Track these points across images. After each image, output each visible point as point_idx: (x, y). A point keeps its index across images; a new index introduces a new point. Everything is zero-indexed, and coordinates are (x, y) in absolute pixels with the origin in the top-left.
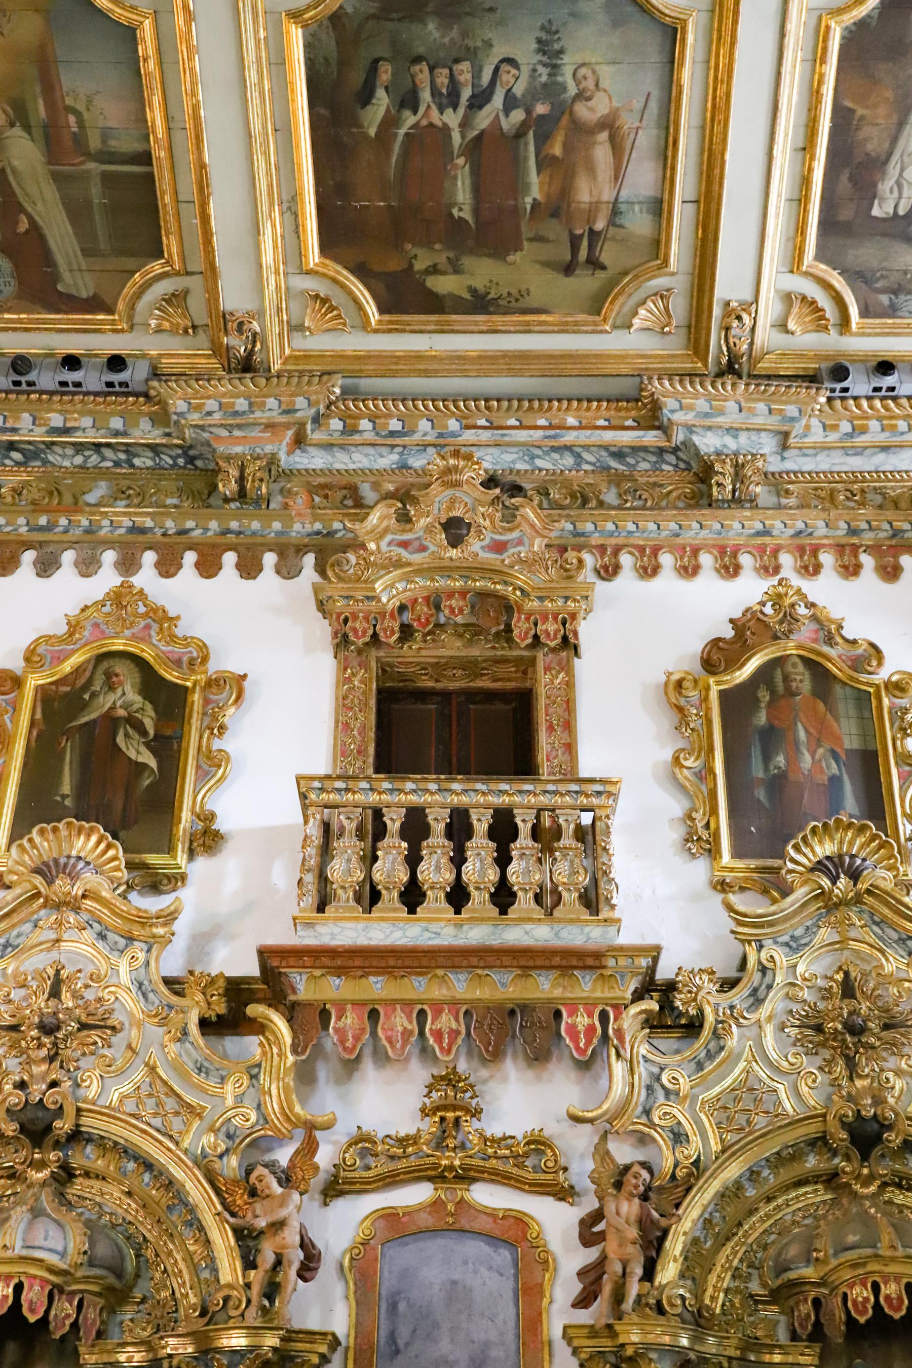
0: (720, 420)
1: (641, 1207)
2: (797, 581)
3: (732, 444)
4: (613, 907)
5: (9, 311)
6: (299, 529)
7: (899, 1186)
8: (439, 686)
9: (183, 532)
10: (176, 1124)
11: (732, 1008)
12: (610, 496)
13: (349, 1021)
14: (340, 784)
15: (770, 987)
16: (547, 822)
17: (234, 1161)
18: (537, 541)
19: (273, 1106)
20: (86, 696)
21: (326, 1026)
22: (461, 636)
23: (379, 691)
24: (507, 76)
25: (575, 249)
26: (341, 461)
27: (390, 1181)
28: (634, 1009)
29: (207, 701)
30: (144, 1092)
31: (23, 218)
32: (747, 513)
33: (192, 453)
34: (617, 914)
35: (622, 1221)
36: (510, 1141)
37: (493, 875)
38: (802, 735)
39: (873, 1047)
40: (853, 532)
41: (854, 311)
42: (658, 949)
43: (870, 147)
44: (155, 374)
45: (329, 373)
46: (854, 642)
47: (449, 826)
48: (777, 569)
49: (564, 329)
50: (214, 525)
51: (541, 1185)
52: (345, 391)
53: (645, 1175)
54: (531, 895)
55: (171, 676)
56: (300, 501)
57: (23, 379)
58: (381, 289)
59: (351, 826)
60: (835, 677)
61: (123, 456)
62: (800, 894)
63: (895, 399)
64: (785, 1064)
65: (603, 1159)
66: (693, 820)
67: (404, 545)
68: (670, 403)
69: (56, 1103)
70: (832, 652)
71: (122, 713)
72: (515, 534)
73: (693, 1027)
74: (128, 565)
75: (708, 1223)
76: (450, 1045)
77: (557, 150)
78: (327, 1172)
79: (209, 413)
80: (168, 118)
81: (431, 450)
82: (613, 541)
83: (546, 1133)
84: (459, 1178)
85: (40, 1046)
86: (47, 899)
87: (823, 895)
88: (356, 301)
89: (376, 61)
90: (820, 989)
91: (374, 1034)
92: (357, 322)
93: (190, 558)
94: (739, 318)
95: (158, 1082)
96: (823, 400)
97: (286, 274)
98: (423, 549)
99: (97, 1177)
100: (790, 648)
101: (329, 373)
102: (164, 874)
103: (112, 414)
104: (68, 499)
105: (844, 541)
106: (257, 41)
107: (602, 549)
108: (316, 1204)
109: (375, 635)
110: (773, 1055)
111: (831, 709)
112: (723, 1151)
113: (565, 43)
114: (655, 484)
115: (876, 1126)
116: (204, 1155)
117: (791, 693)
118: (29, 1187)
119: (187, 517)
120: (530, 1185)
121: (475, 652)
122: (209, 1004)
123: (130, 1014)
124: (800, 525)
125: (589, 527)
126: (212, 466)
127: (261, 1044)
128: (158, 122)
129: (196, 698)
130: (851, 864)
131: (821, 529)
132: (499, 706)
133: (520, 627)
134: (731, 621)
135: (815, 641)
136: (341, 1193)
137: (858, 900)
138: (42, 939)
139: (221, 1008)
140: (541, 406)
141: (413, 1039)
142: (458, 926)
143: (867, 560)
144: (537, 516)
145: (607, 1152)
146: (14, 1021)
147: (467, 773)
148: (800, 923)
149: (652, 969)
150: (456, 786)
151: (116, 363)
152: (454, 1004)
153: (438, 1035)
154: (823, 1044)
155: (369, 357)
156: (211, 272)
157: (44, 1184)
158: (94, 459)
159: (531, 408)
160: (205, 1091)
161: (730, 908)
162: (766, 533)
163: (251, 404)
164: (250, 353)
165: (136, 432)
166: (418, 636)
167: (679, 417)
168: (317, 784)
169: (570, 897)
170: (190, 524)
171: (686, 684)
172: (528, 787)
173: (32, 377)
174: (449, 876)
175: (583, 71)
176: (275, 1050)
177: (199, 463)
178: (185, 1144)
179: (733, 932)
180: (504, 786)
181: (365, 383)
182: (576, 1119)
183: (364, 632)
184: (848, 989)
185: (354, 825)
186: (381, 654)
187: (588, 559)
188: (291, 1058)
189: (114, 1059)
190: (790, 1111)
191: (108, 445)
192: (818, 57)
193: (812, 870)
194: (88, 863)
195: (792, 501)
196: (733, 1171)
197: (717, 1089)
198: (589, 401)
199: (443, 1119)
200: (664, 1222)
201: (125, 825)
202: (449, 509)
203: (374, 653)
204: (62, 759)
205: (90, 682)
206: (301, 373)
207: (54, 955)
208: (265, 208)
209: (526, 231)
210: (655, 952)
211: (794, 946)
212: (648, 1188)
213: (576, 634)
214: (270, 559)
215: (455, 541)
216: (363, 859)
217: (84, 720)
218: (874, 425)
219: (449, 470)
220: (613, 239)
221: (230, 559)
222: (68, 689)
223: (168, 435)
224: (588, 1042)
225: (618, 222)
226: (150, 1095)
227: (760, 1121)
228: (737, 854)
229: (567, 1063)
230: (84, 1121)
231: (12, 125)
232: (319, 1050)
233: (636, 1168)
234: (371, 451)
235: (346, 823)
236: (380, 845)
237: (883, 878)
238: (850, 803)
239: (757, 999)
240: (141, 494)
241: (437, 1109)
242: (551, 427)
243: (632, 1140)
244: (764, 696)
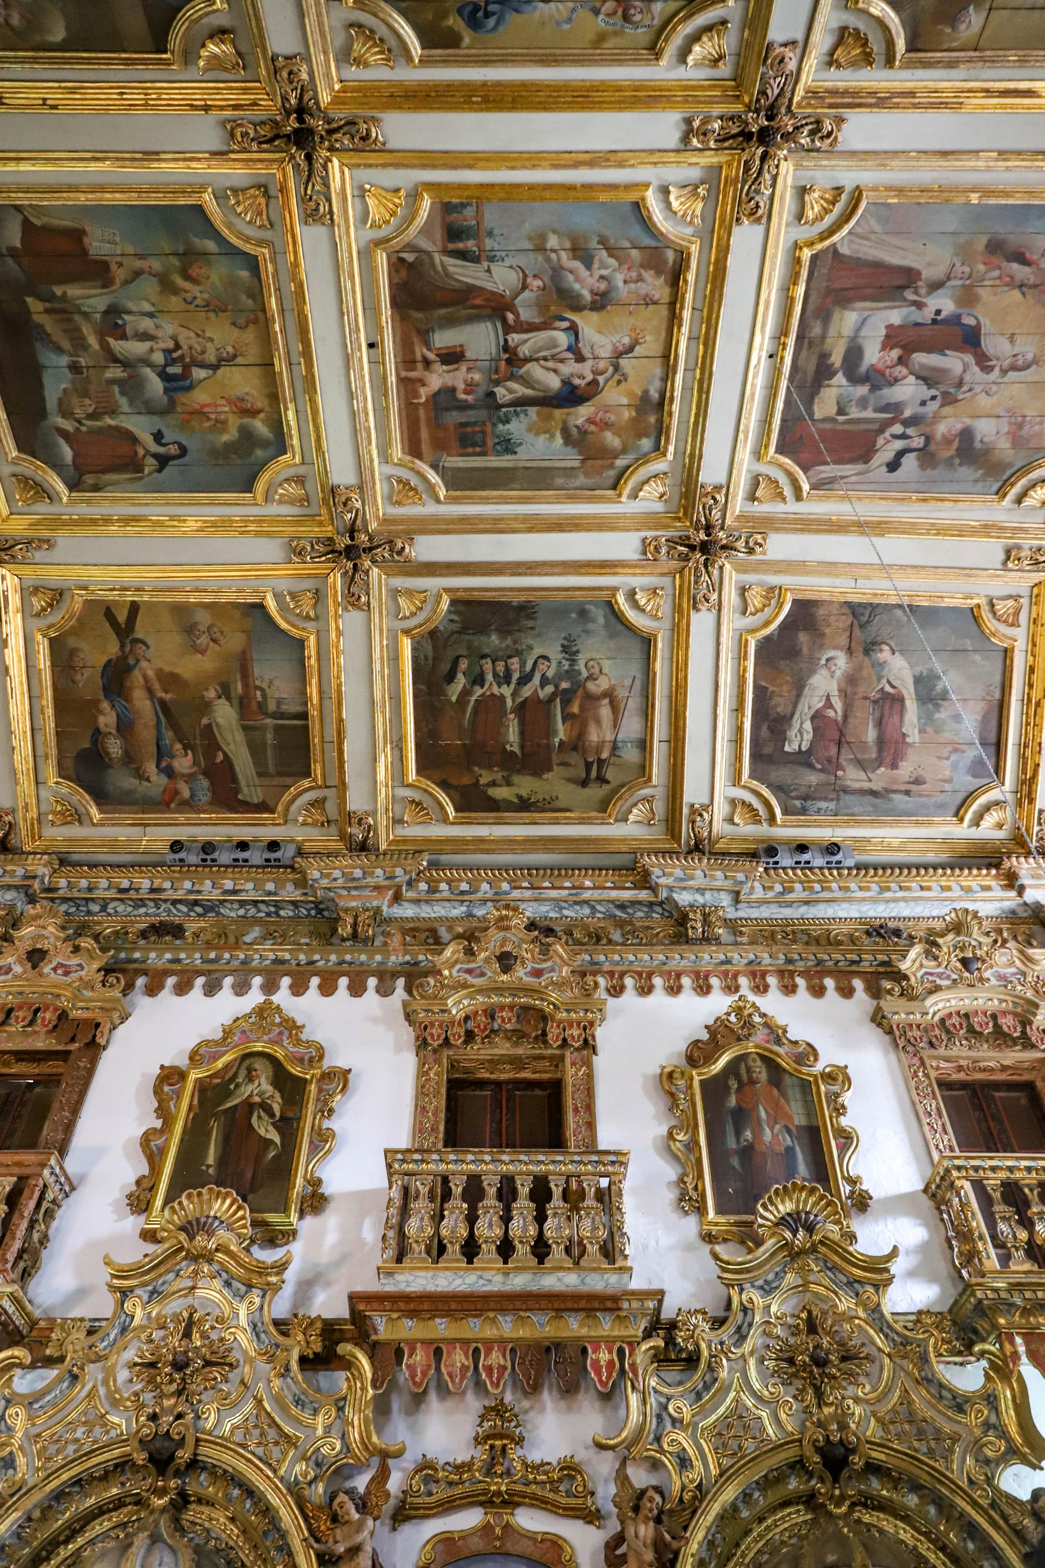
0: (691, 883)
1: (656, 1529)
2: (752, 997)
3: (701, 900)
4: (626, 1257)
5: (204, 812)
6: (395, 959)
7: (865, 1506)
8: (493, 1077)
9: (311, 963)
10: (276, 1452)
11: (722, 1343)
12: (616, 936)
13: (418, 1358)
14: (417, 1157)
15: (750, 1325)
16: (574, 1186)
17: (320, 1488)
18: (565, 969)
19: (354, 1435)
20: (232, 1087)
21: (399, 1362)
22: (509, 1039)
23: (449, 1081)
24: (542, 666)
25: (588, 771)
26: (426, 912)
27: (448, 1507)
28: (644, 1347)
29: (320, 1090)
30: (250, 1424)
31: (220, 754)
32: (714, 948)
33: (321, 906)
34: (629, 1263)
35: (641, 1544)
36: (547, 1467)
37: (532, 1231)
38: (763, 1114)
39: (835, 1377)
40: (789, 961)
41: (778, 811)
42: (662, 1293)
43: (779, 710)
44: (300, 853)
45: (420, 852)
46: (796, 1043)
47: (499, 1190)
48: (737, 989)
49: (582, 821)
50: (333, 958)
51: (573, 1509)
52: (432, 864)
53: (658, 1498)
54: (562, 1247)
55: (295, 1070)
56: (396, 940)
57: (209, 857)
58: (457, 796)
59: (424, 1190)
60: (784, 1070)
61: (272, 909)
62: (769, 1244)
63: (811, 869)
64: (766, 1393)
65: (623, 1484)
66: (685, 1183)
67: (469, 971)
68: (657, 872)
69: (179, 1434)
70: (780, 1050)
71: (257, 1099)
72: (549, 964)
73: (692, 1361)
74: (270, 987)
75: (711, 1544)
76: (499, 1379)
77: (575, 709)
78: (396, 1497)
79: (335, 879)
80: (321, 692)
81: (489, 904)
82: (619, 968)
83: (576, 1459)
84: (505, 1503)
85: (171, 1381)
86: (188, 1251)
87: (787, 1246)
88: (440, 804)
89: (458, 657)
90: (790, 1326)
91: (438, 1369)
92: (440, 817)
93: (315, 981)
94: (701, 815)
95: (263, 1413)
96: (761, 869)
97: (393, 787)
98: (483, 974)
99: (208, 1503)
100: (750, 1047)
101: (420, 852)
102: (281, 1231)
103: (268, 880)
104: (232, 940)
105: (784, 968)
106: (382, 647)
107: (611, 974)
108: (387, 1529)
109: (446, 1039)
110: (757, 1386)
111: (783, 1094)
112: (721, 1475)
113: (579, 647)
114: (648, 928)
115: (842, 1450)
116: (297, 1482)
117: (752, 1082)
118: (152, 1512)
119: (314, 951)
120: (564, 1509)
121: (520, 1051)
122: (308, 1343)
123: (245, 1352)
124: (752, 957)
125: (602, 958)
126: (334, 915)
127: (348, 1379)
128: (314, 695)
129: (313, 1087)
130: (806, 1220)
131: (766, 960)
132: (538, 1092)
133: (553, 1032)
134: (706, 1027)
135: (768, 1042)
136: (408, 1518)
137: (814, 1249)
138: (181, 1286)
139: (317, 1347)
140: (566, 874)
141: (469, 1374)
142: (506, 1274)
143: (800, 982)
144: (565, 951)
145: (627, 1477)
146: (152, 1359)
147: (514, 1147)
148: (771, 1269)
149: (658, 1310)
150: (505, 1158)
151: (273, 846)
152: (502, 1342)
153: (489, 1369)
154: (795, 1375)
155: (448, 840)
156: (342, 786)
157: (163, 1510)
158: (252, 911)
159: (559, 875)
160: (300, 1422)
161: (716, 1257)
162: (728, 962)
163: (364, 873)
164: (366, 839)
165: (283, 893)
166: (478, 1039)
167: (663, 881)
168: (399, 1156)
169: (593, 1249)
170: (316, 957)
171: (675, 1075)
172: (560, 1158)
173: (215, 856)
174: (498, 1231)
175: (591, 663)
176: (359, 1385)
177: (326, 913)
178: (282, 1472)
179: (719, 1277)
180: (541, 1158)
181: (444, 858)
182: (601, 1447)
183: (439, 1036)
184: (812, 1327)
185: (427, 1189)
186: (451, 1053)
187: (601, 981)
188: (371, 1392)
189: (229, 1394)
190: (774, 1438)
191: (263, 902)
192: (741, 655)
193: (777, 1225)
194: (222, 1222)
195: (745, 939)
196: (730, 1494)
197: (714, 1417)
198: (600, 870)
199: (492, 1447)
200: (675, 1545)
201: (253, 1190)
202: (502, 946)
203: (446, 1052)
204: (209, 1135)
205: (235, 1075)
206: (400, 852)
207: (190, 1300)
208: (381, 745)
209: (555, 758)
210: (659, 1295)
211: (767, 1289)
212: (661, 1512)
213: (594, 1039)
214: (372, 982)
215: (506, 969)
216: (432, 1217)
217: (228, 1105)
218: (798, 886)
219: (502, 918)
220: (614, 764)
221: (343, 982)
222: (218, 1081)
223: (305, 894)
224: (609, 1377)
226: (256, 1426)
227: (749, 1445)
228: (719, 1211)
229: (592, 1392)
230: (202, 1450)
231: (219, 697)
232: (393, 1384)
233: (651, 1493)
234: (447, 904)
235: (420, 1187)
236: (446, 1206)
237: (833, 1231)
238: (802, 1168)
239: (741, 1337)
240: (283, 936)
241: (488, 1437)
242: (573, 888)
243: (647, 1465)
244: (733, 1084)
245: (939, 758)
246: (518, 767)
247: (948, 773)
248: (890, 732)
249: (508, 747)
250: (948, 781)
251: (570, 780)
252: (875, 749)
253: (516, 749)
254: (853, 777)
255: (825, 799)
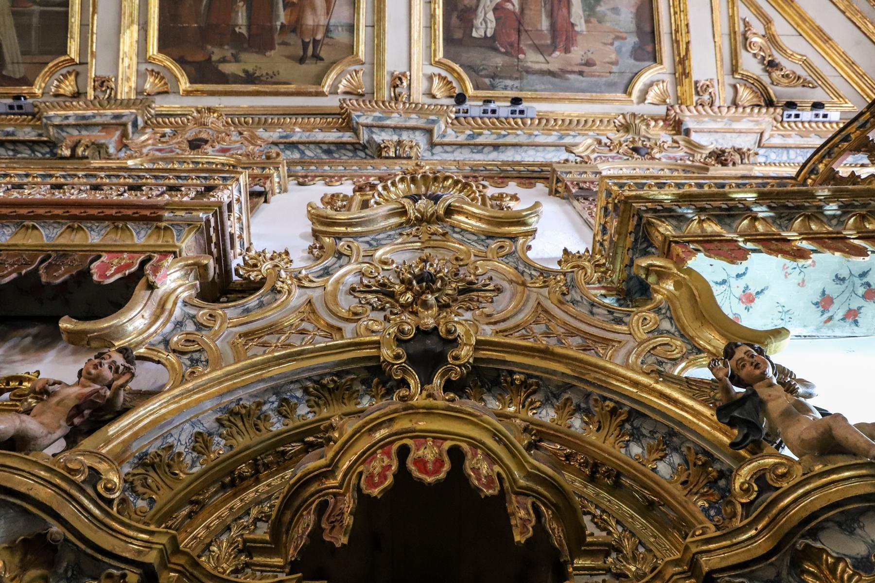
220: (327, 44)
225: (329, 35)
245: (605, 44)
246: (246, 46)
247: (613, 57)
248: (560, 21)
249: (237, 29)
250: (615, 63)
251: (290, 57)
252: (549, 36)
253: (244, 31)
254: (533, 59)
255: (511, 78)
